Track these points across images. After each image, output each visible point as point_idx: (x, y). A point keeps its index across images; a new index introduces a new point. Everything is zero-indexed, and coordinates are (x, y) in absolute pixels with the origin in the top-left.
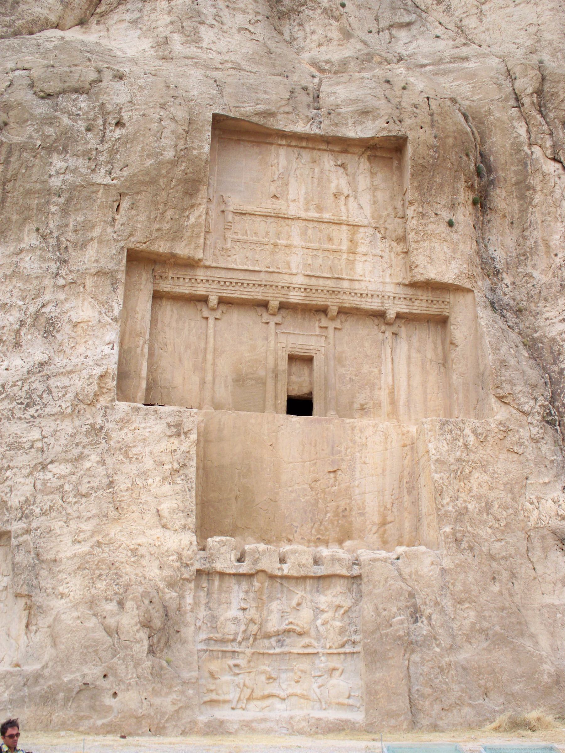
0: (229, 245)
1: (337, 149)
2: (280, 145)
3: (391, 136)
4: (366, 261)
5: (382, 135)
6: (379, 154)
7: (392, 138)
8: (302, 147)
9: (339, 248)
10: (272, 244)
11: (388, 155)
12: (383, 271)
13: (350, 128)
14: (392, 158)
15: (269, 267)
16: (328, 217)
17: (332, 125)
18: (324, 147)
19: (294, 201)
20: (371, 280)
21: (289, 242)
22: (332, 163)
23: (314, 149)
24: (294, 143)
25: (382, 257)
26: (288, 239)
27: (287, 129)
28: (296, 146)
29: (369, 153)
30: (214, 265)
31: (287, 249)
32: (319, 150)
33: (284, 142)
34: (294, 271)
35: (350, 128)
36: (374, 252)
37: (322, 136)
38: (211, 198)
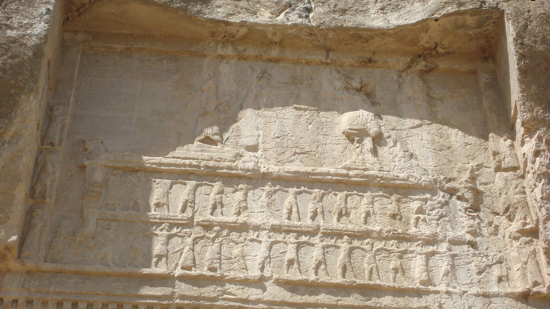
0: (91, 228)
1: (348, 60)
2: (222, 57)
3: (465, 12)
4: (433, 253)
5: (444, 12)
6: (443, 65)
7: (470, 20)
8: (270, 60)
9: (364, 227)
10: (198, 224)
11: (466, 67)
12: (480, 273)
13: (373, 16)
14: (474, 72)
15: (189, 269)
16: (332, 171)
17: (334, 12)
18: (320, 57)
19: (254, 148)
20: (450, 289)
21: (241, 219)
22: (339, 84)
23: (297, 62)
24: (252, 51)
25: (472, 245)
26: (239, 214)
27: (232, 19)
28: (258, 58)
29: (421, 65)
30: (48, 266)
31: (234, 235)
32: (308, 63)
33: (229, 51)
34: (254, 273)
35: (373, 16)
36: (451, 234)
37: (311, 31)
38: (56, 142)
